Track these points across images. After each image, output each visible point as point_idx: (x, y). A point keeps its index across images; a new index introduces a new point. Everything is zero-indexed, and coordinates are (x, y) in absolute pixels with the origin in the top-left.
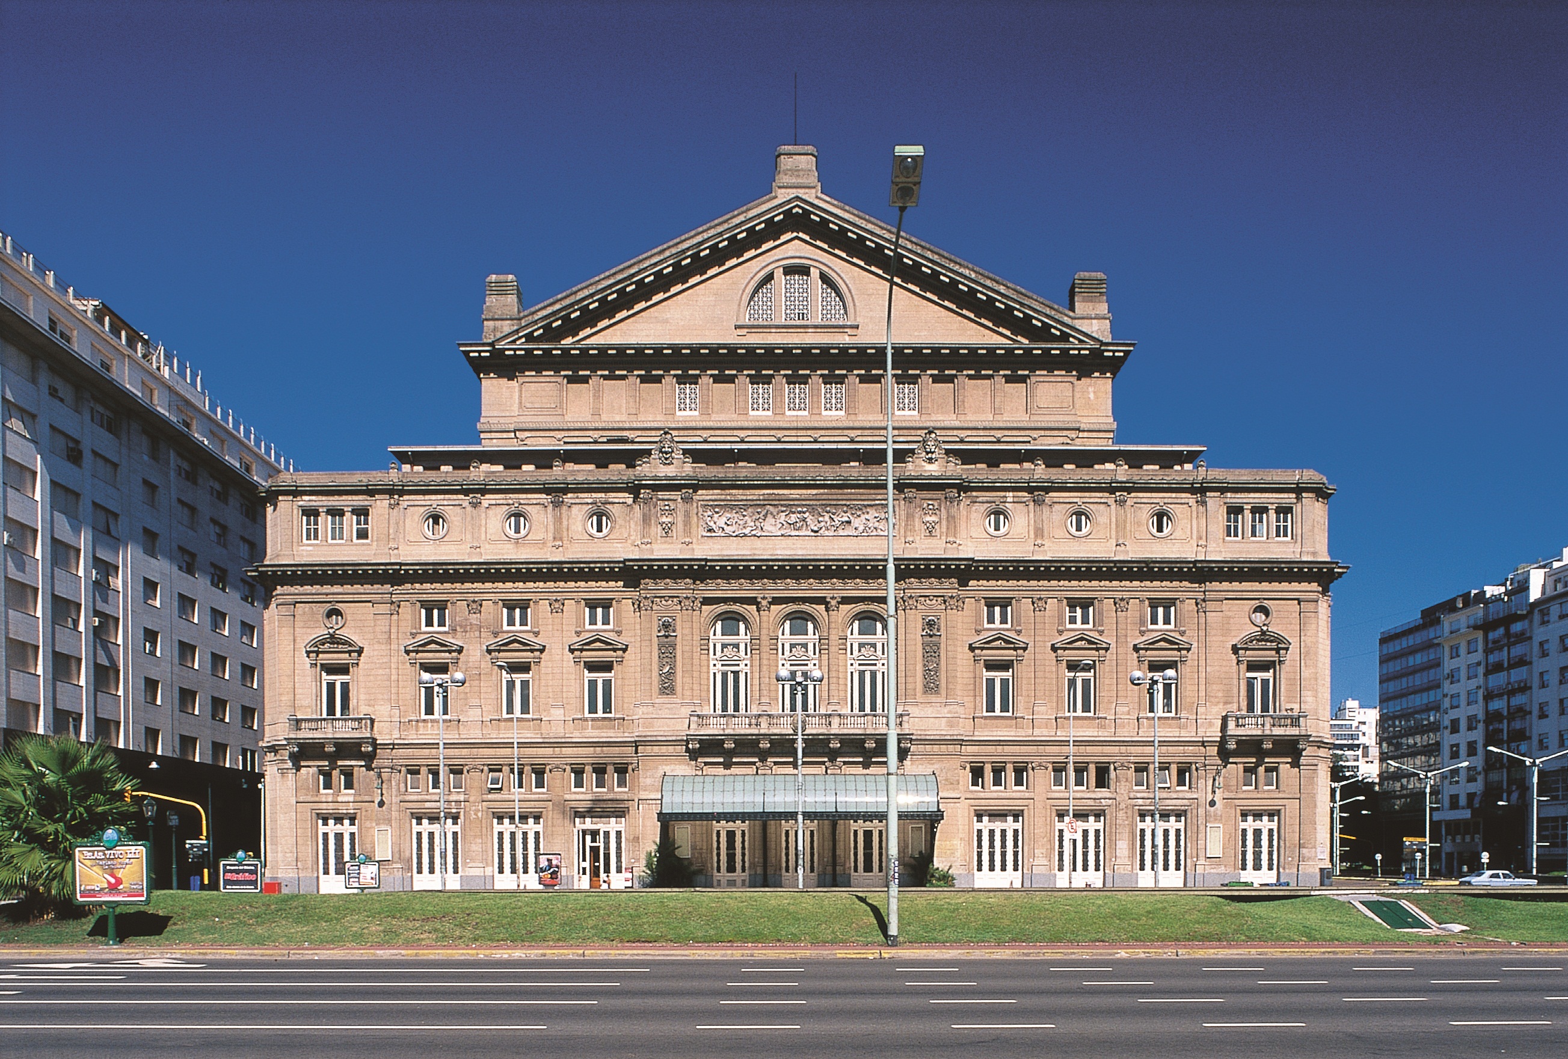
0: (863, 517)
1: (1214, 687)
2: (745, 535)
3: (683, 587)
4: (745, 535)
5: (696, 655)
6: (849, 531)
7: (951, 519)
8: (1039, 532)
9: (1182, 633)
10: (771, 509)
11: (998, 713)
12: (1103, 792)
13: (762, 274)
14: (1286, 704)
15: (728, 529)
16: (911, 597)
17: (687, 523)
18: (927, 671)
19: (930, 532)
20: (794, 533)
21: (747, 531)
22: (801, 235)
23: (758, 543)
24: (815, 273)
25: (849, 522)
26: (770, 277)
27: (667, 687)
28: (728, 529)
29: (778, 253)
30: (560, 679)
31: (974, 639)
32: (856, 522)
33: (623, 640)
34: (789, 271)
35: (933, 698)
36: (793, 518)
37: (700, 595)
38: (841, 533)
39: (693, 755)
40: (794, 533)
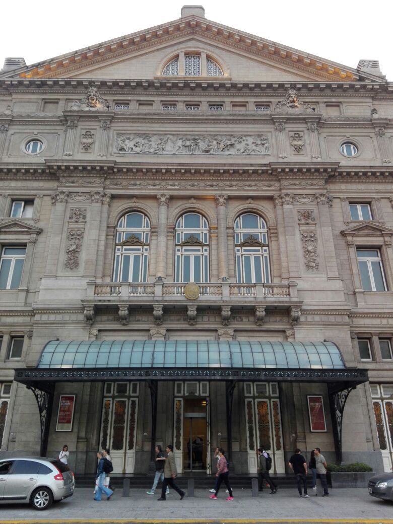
0: (243, 143)
3: (95, 185)
10: (171, 137)
13: (172, 55)
15: (138, 149)
16: (287, 195)
21: (152, 150)
24: (204, 56)
25: (232, 145)
26: (177, 57)
28: (138, 149)
31: (344, 228)
33: (40, 225)
34: (188, 55)
37: (110, 192)
39: (90, 321)
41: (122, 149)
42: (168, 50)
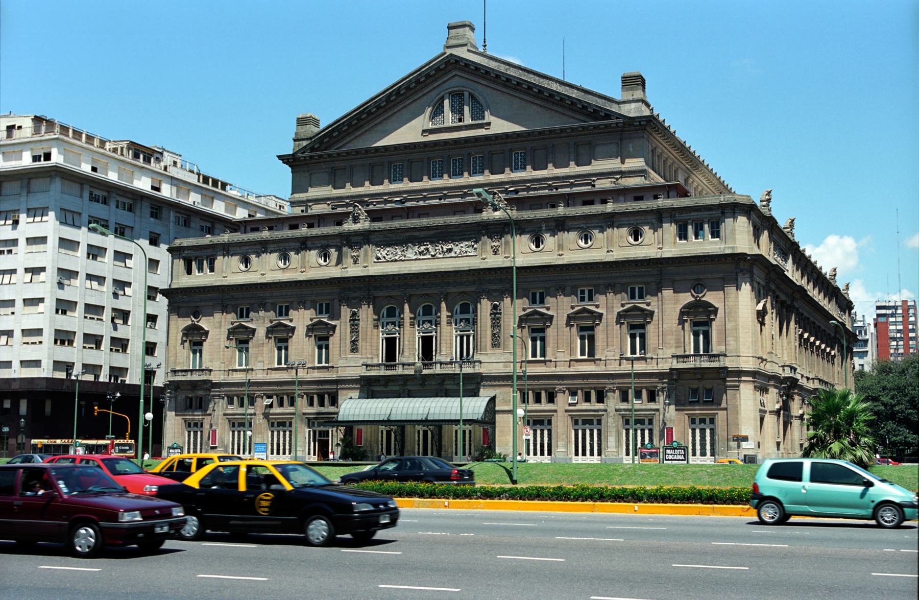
1: (668, 337)
2: (396, 261)
4: (396, 261)
5: (369, 330)
6: (453, 254)
7: (507, 243)
8: (560, 247)
9: (648, 304)
11: (538, 358)
12: (601, 406)
14: (716, 349)
17: (366, 254)
18: (494, 335)
19: (495, 253)
20: (422, 257)
22: (460, 74)
23: (402, 264)
24: (466, 94)
25: (450, 250)
27: (354, 349)
29: (446, 86)
30: (302, 347)
32: (457, 249)
35: (497, 351)
36: (422, 248)
38: (447, 255)
40: (422, 257)
41: (378, 258)
42: (434, 93)
